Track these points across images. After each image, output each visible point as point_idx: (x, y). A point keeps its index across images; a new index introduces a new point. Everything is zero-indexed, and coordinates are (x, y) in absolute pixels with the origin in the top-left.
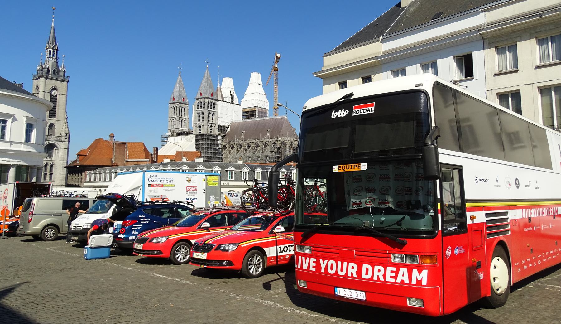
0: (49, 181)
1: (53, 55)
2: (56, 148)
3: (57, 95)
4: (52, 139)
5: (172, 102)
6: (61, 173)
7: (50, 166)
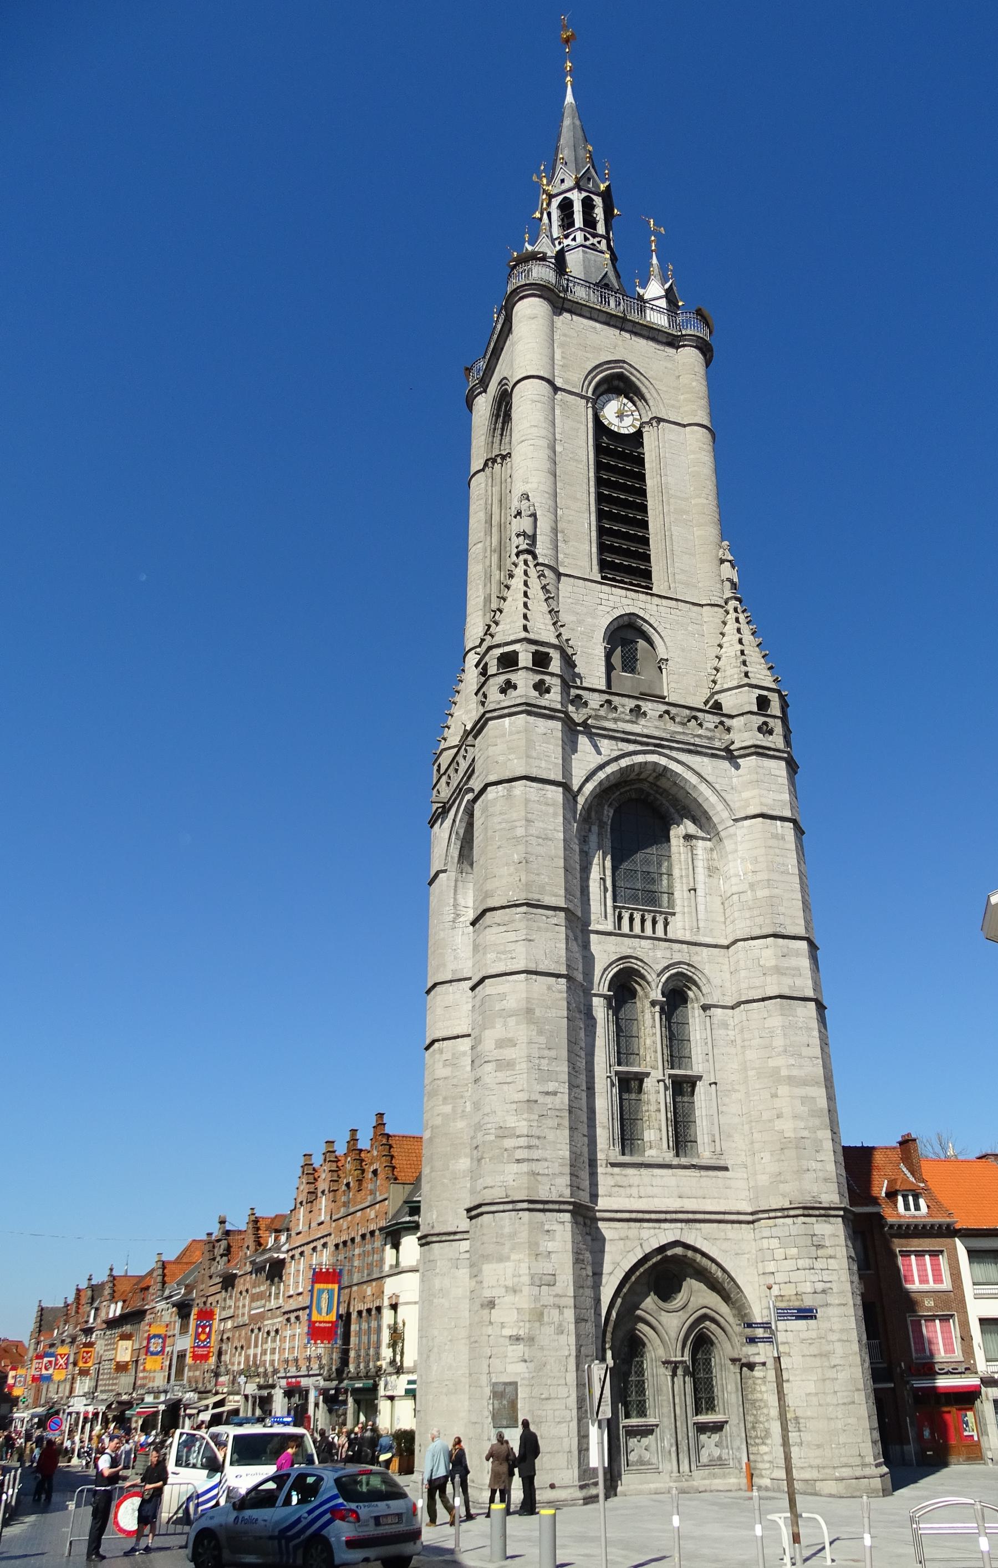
0: (669, 1157)
1: (590, 222)
2: (688, 827)
4: (656, 734)
6: (780, 1061)
7: (657, 995)
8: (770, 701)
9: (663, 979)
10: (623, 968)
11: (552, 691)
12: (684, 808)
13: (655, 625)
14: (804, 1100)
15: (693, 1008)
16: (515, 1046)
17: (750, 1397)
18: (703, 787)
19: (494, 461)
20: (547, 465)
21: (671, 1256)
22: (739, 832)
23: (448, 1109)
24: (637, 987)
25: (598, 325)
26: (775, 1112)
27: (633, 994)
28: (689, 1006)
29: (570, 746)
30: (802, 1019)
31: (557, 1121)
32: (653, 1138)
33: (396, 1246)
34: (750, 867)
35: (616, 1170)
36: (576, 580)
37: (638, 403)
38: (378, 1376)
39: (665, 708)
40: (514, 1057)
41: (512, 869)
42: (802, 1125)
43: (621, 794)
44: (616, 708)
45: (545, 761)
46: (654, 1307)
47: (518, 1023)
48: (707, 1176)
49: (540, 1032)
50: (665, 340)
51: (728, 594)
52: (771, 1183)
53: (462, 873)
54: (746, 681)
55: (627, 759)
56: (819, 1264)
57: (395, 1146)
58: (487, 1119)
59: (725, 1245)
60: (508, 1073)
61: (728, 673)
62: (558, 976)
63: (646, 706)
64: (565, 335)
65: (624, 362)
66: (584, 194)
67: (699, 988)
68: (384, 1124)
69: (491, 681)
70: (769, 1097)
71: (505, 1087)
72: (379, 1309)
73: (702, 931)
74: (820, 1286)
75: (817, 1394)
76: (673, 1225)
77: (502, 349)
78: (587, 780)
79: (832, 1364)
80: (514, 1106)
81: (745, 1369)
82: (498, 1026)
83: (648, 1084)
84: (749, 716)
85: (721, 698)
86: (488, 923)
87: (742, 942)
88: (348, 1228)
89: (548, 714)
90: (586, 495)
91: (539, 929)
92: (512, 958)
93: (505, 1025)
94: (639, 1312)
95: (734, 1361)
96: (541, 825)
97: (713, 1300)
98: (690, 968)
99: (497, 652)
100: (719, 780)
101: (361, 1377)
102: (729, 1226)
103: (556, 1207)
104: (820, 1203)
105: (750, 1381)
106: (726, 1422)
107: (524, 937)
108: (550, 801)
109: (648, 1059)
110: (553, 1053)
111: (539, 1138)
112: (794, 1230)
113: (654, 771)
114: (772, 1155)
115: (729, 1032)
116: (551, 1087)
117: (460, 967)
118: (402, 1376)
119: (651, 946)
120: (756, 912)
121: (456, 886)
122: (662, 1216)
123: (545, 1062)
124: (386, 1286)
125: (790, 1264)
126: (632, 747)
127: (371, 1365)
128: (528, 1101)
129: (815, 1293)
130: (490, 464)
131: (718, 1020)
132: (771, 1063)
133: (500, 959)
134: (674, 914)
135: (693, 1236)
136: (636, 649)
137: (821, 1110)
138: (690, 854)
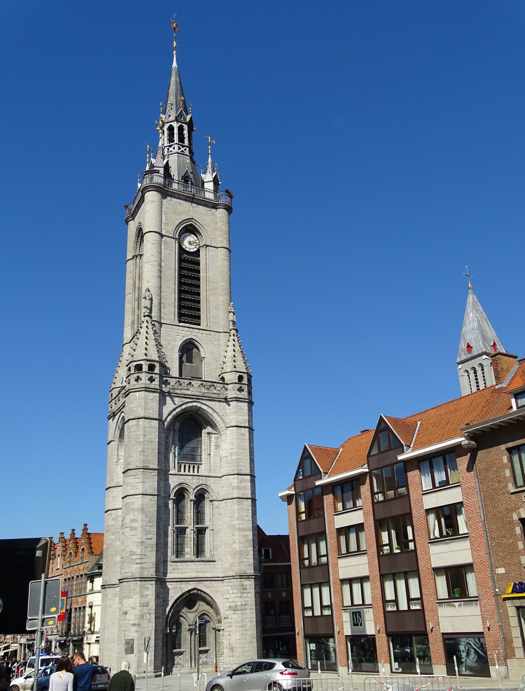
0: (194, 558)
1: (181, 139)
2: (209, 429)
3: (198, 251)
4: (197, 394)
5: (464, 357)
6: (236, 522)
7: (192, 497)
8: (243, 377)
9: (195, 491)
10: (180, 488)
11: (156, 380)
12: (208, 421)
13: (200, 343)
14: (244, 536)
15: (207, 501)
16: (137, 522)
17: (218, 641)
18: (215, 415)
19: (137, 257)
20: (157, 274)
21: (193, 593)
22: (228, 432)
23: (113, 537)
24: (185, 494)
25: (182, 201)
26: (233, 541)
27: (184, 497)
28: (205, 500)
29: (162, 403)
30: (245, 506)
31: (151, 549)
32: (188, 551)
33: (92, 582)
34: (231, 446)
35: (174, 564)
36: (168, 325)
37: (199, 236)
38: (84, 635)
39: (201, 382)
40: (137, 526)
41: (138, 454)
42: (242, 545)
43: (183, 417)
44: (181, 384)
45: (152, 410)
46: (186, 611)
47: (138, 514)
48: (208, 564)
49: (146, 517)
50: (211, 206)
51: (231, 327)
52: (230, 566)
53: (120, 442)
54: (234, 369)
55: (185, 405)
56: (244, 595)
57: (92, 538)
58: (126, 548)
59: (213, 589)
60: (135, 532)
61: (228, 365)
62: (154, 495)
63: (194, 382)
64: (167, 208)
65: (193, 219)
66: (180, 124)
67: (208, 493)
68: (87, 529)
69: (132, 376)
70: (231, 535)
71: (133, 537)
72: (84, 607)
73: (211, 471)
74: (244, 603)
75: (239, 640)
76: (193, 583)
77: (141, 206)
78: (169, 415)
79: (246, 629)
80: (136, 544)
81: (217, 631)
82: (131, 514)
83: (188, 531)
84: (234, 384)
85: (225, 376)
86: (129, 475)
87: (226, 476)
88: (71, 572)
89: (153, 391)
90: (174, 285)
91: (147, 478)
92: (137, 489)
93: (134, 513)
94: (181, 613)
95: (213, 629)
96: (150, 436)
97: (207, 608)
98: (206, 486)
99: (135, 363)
100: (221, 411)
101: (76, 635)
102: (214, 582)
103: (150, 579)
104: (247, 574)
105: (218, 636)
106: (209, 650)
107: (141, 481)
108: (153, 426)
109: (188, 521)
110: (151, 524)
111: (145, 555)
112: (236, 583)
113: (196, 408)
114: (231, 557)
115: (220, 510)
116: (150, 536)
117: (119, 481)
118: (94, 635)
119: (192, 478)
120: (232, 465)
121: (118, 448)
122: (190, 580)
123: (148, 527)
124: (87, 598)
125: (234, 595)
126: (187, 400)
127: (81, 630)
128: (141, 542)
129: (242, 605)
130: (135, 257)
131: (216, 506)
132: (233, 523)
133: (133, 489)
134: (201, 464)
135: (201, 586)
136: (193, 352)
137: (250, 540)
138: (209, 440)
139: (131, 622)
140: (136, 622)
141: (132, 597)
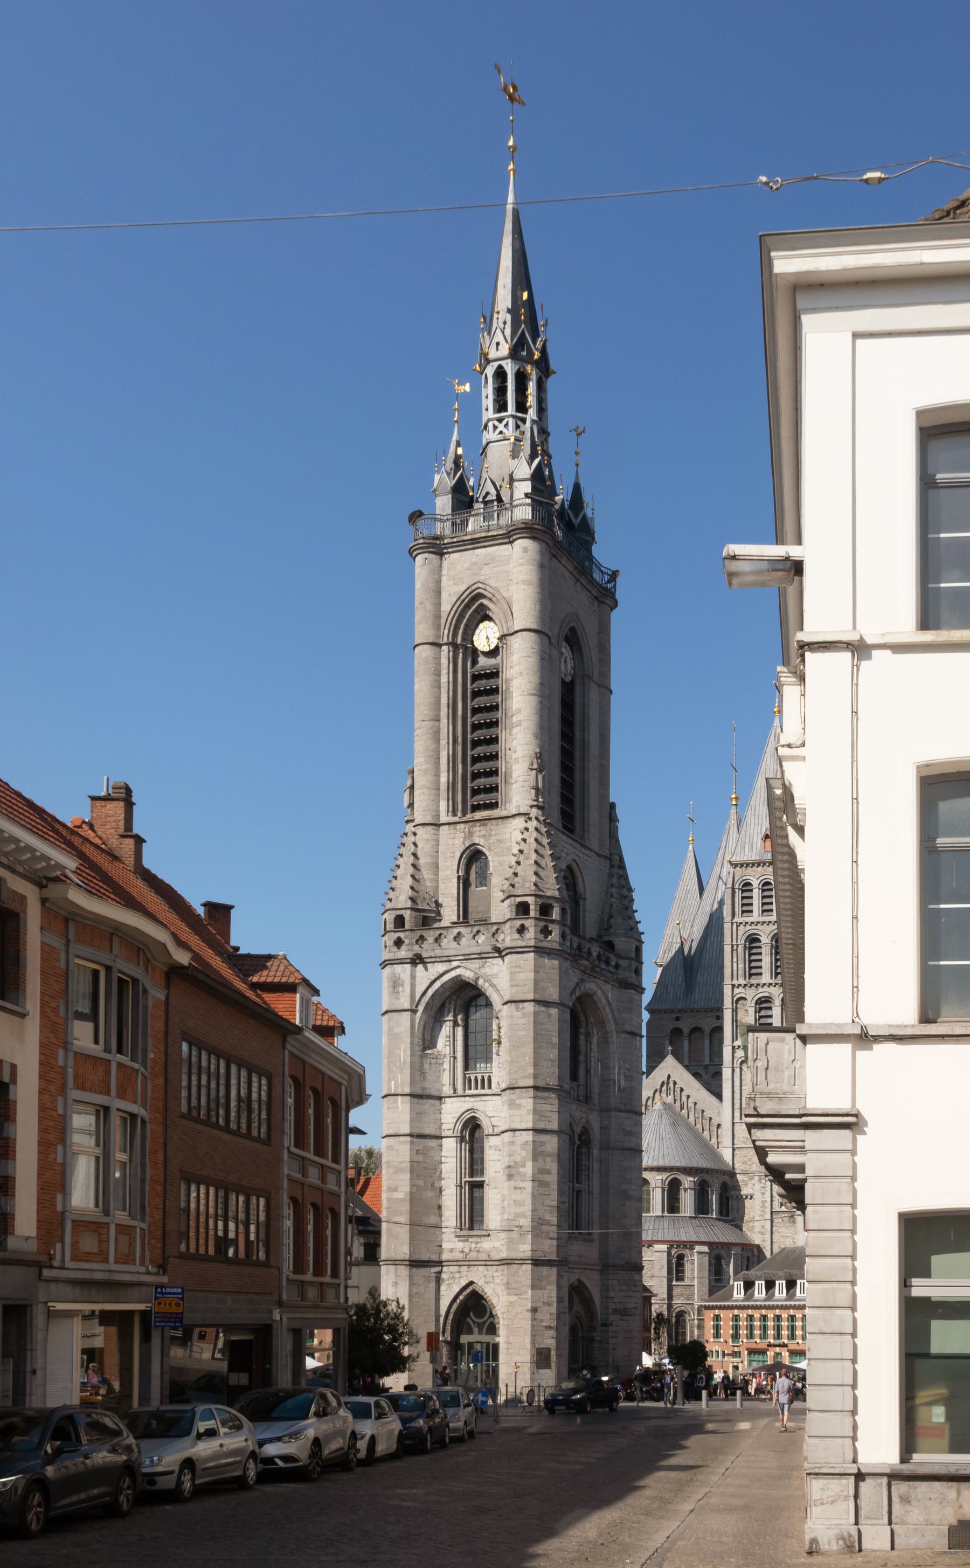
16: (550, 1174)
41: (549, 1064)
71: (544, 1197)
80: (549, 1208)
82: (540, 1161)
93: (544, 1161)
133: (541, 1121)
139: (544, 1324)
140: (552, 1325)
141: (545, 1288)
